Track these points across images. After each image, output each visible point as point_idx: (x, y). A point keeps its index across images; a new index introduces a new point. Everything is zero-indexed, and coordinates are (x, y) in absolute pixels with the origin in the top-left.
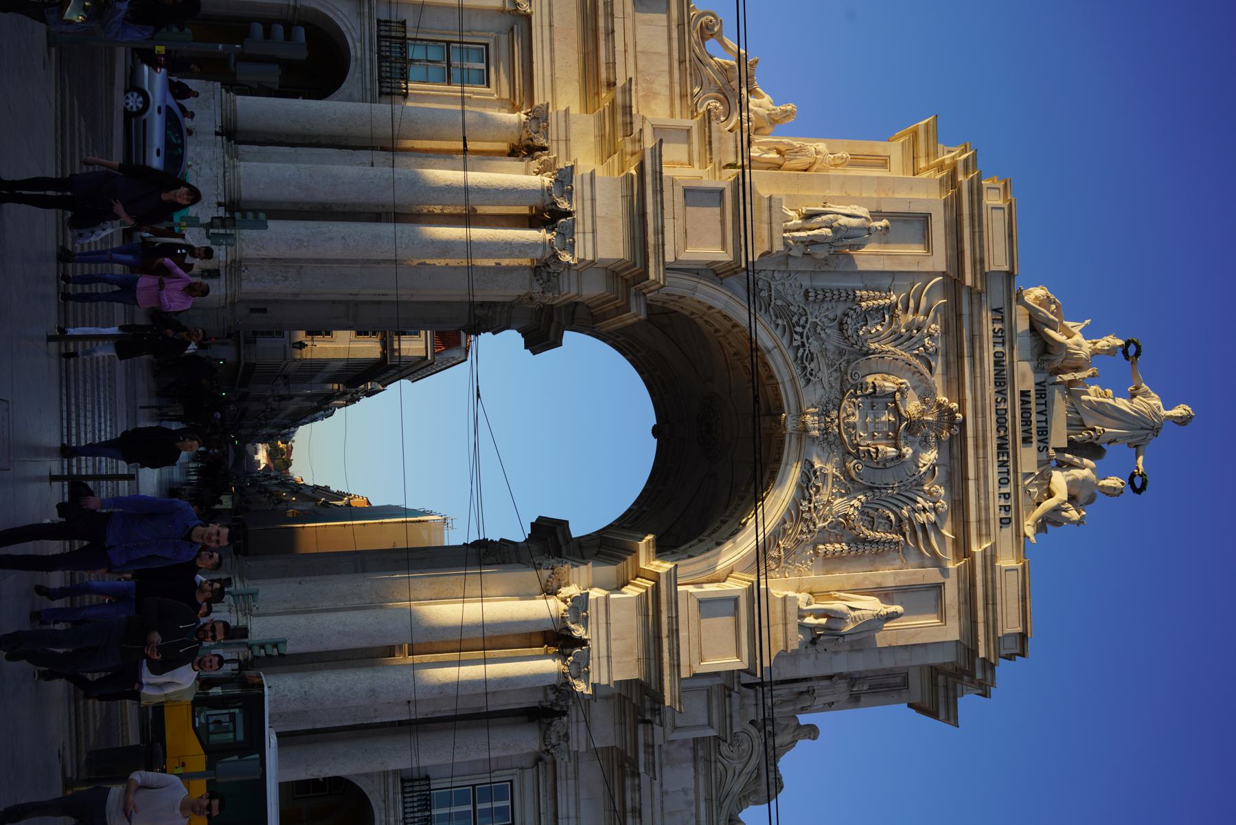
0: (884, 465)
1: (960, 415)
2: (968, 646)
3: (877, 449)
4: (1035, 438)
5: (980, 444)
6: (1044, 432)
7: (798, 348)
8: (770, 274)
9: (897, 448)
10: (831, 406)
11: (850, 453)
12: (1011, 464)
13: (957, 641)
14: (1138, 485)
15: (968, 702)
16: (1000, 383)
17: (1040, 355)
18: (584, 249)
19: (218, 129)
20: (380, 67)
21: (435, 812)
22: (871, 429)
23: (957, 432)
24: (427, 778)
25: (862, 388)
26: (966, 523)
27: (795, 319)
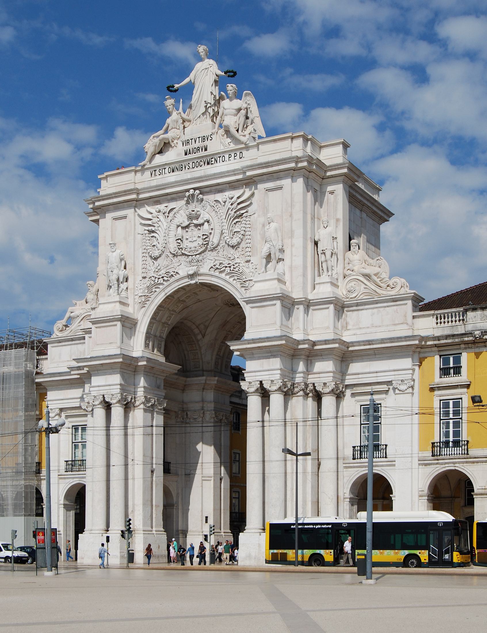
3: (203, 235)
6: (204, 139)
7: (164, 280)
8: (136, 297)
9: (204, 224)
10: (188, 260)
11: (207, 248)
14: (232, 74)
16: (181, 168)
25: (179, 246)
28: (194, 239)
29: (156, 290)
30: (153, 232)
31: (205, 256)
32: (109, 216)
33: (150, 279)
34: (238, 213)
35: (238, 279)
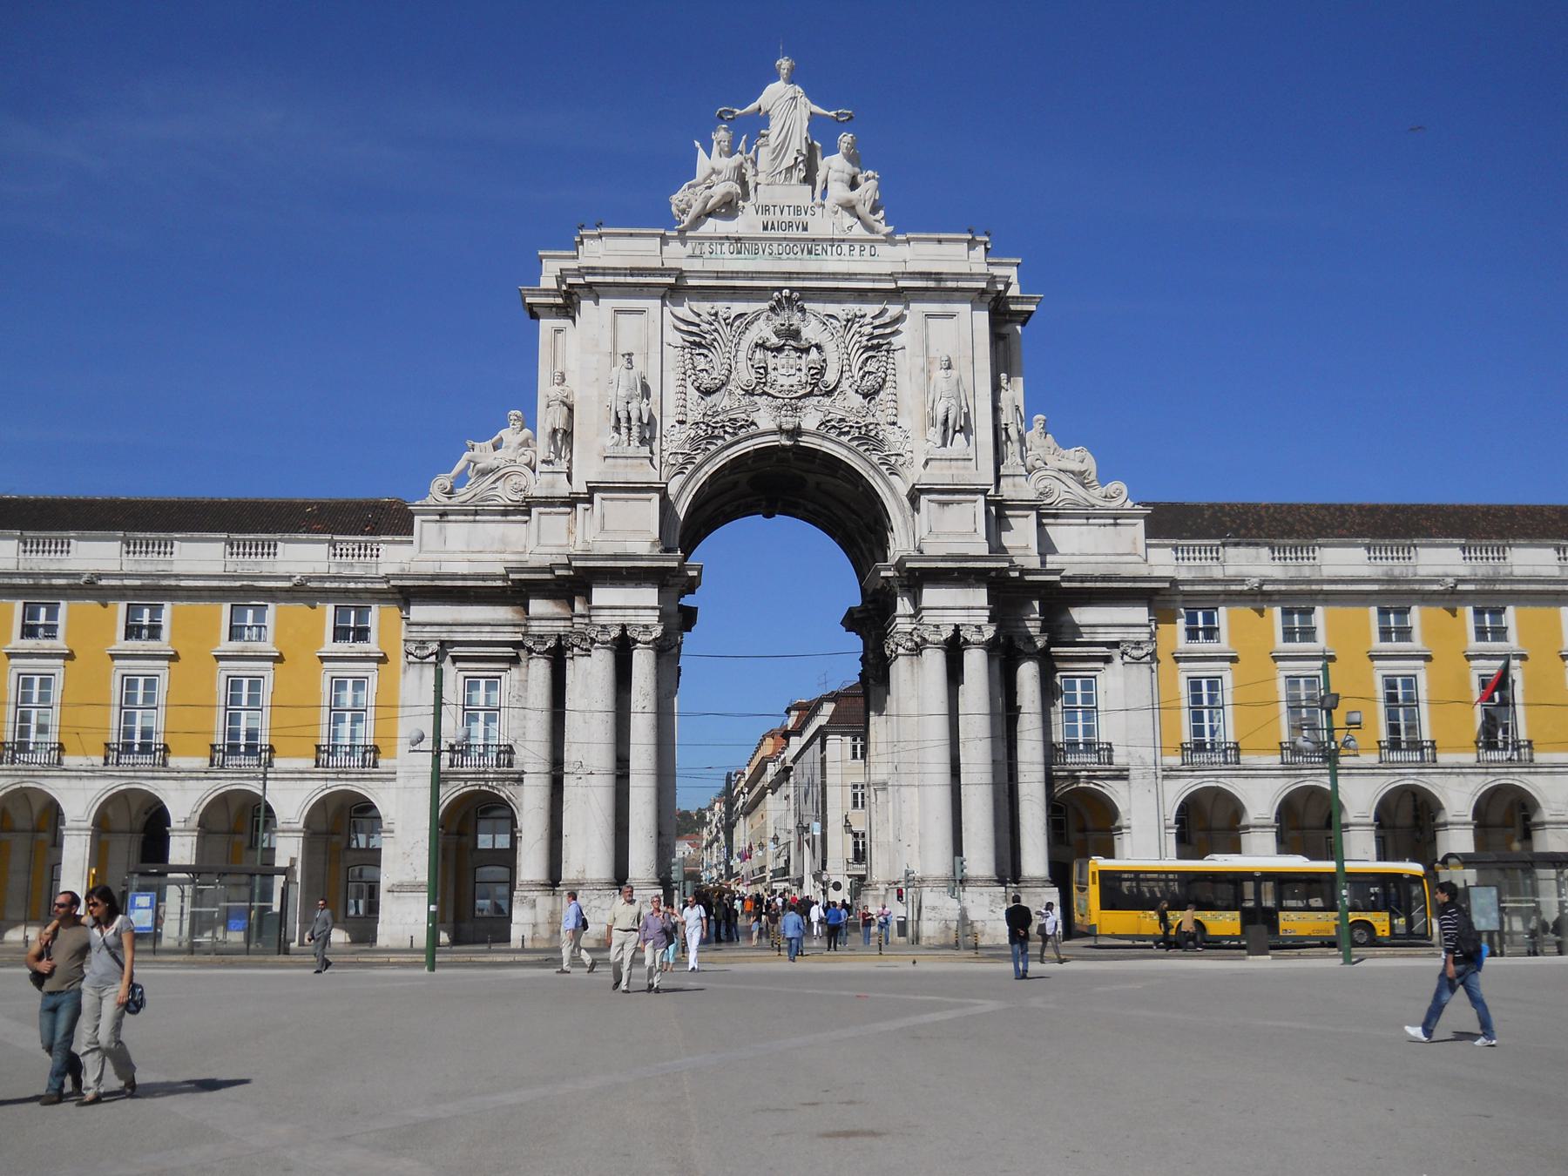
0: (824, 361)
1: (784, 291)
2: (978, 297)
3: (812, 368)
6: (798, 210)
11: (813, 390)
13: (971, 302)
18: (651, 618)
21: (1081, 739)
28: (793, 371)
30: (700, 345)
31: (807, 403)
32: (608, 304)
34: (875, 342)
35: (874, 450)
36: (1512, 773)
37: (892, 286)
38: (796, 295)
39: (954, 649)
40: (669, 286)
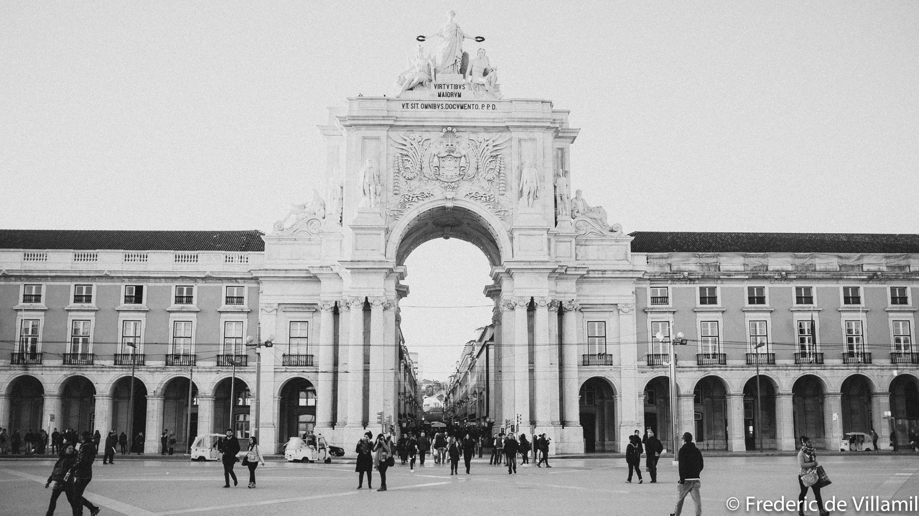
1: (449, 127)
4: (459, 90)
5: (460, 119)
6: (456, 87)
7: (418, 199)
10: (443, 185)
11: (463, 178)
12: (469, 103)
15: (572, 123)
17: (423, 85)
19: (332, 429)
20: (301, 366)
22: (452, 168)
23: (456, 130)
24: (584, 355)
26: (494, 127)
27: (406, 200)
28: (451, 169)
29: (410, 206)
33: (404, 196)
36: (813, 369)
37: (504, 125)
38: (454, 130)
39: (532, 307)
40: (391, 126)
